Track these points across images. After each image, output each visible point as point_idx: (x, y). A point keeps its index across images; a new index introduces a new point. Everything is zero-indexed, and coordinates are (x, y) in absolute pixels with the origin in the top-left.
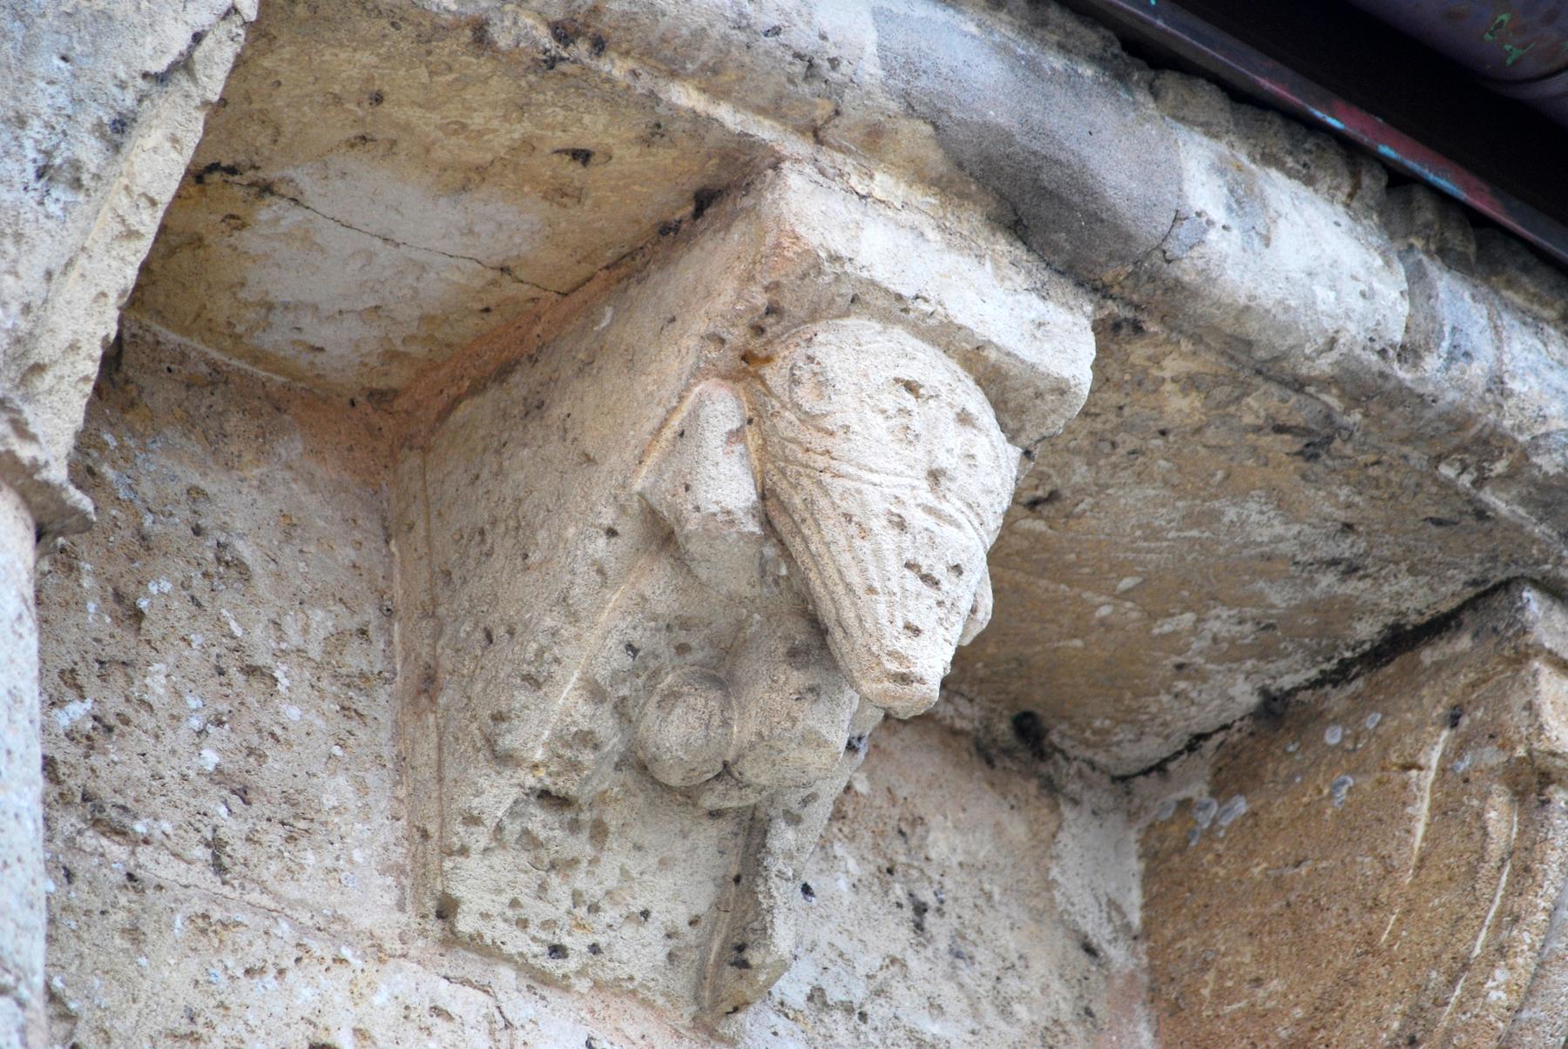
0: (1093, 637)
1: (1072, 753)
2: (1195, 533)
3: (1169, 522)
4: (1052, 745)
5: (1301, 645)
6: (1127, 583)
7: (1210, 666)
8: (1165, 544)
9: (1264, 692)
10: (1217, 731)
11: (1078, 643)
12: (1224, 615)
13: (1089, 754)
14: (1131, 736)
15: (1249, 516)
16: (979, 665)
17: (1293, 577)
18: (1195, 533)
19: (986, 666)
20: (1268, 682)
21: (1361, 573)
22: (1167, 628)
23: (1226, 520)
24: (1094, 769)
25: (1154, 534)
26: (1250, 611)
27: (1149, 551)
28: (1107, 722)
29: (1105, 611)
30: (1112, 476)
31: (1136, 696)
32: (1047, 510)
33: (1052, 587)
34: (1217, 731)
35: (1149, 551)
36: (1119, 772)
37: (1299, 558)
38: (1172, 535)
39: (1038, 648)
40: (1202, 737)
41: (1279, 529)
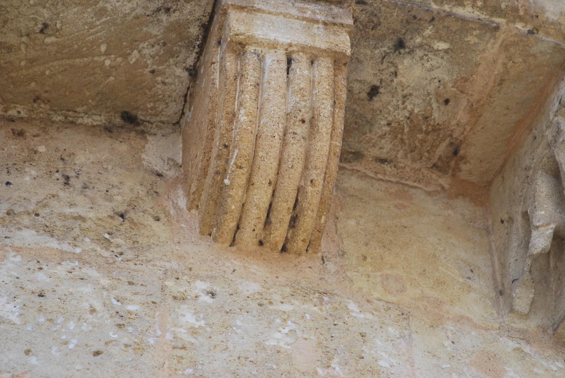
0: (114, 74)
1: (153, 120)
2: (104, 19)
3: (92, 18)
4: (141, 120)
5: (180, 46)
6: (103, 48)
7: (160, 68)
8: (99, 27)
9: (187, 69)
10: (188, 91)
11: (112, 78)
12: (145, 45)
13: (158, 119)
14: (164, 106)
15: (115, 5)
16: (90, 101)
17: (152, 22)
18: (104, 19)
19: (93, 100)
20: (184, 65)
21: (172, 10)
22: (134, 60)
23: (109, 9)
24: (164, 123)
25: (92, 26)
26: (152, 41)
27: (97, 32)
28: (152, 104)
29: (108, 63)
30: (56, 9)
31: (150, 90)
32: (49, 31)
33: (82, 61)
34: (188, 91)
35: (97, 32)
36: (174, 122)
37: (147, 13)
38: (98, 23)
39: (102, 86)
40: (186, 96)
41: (130, 5)
